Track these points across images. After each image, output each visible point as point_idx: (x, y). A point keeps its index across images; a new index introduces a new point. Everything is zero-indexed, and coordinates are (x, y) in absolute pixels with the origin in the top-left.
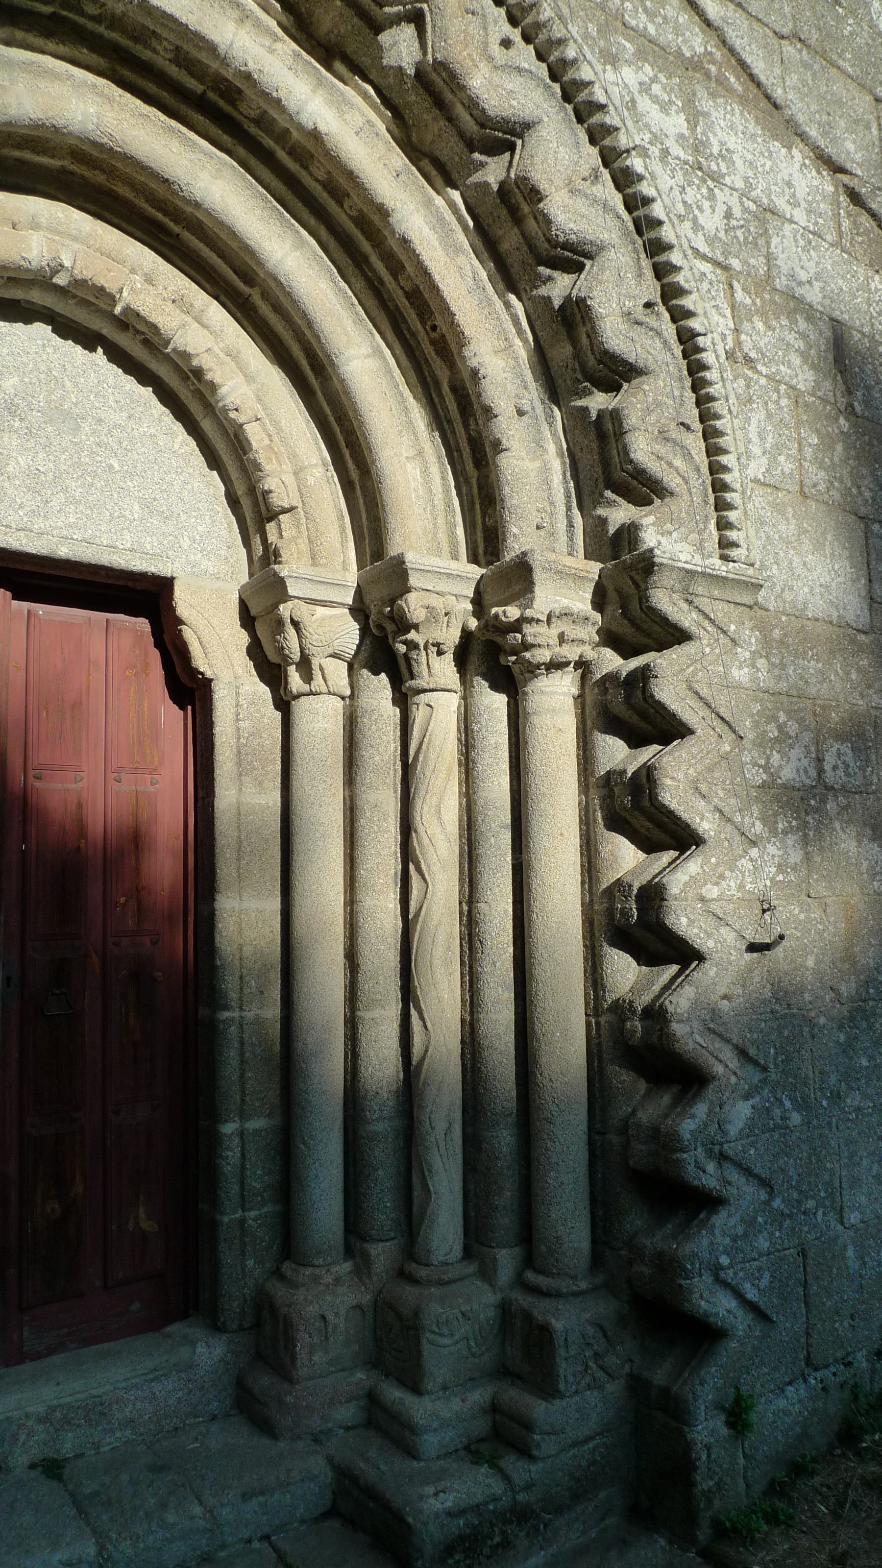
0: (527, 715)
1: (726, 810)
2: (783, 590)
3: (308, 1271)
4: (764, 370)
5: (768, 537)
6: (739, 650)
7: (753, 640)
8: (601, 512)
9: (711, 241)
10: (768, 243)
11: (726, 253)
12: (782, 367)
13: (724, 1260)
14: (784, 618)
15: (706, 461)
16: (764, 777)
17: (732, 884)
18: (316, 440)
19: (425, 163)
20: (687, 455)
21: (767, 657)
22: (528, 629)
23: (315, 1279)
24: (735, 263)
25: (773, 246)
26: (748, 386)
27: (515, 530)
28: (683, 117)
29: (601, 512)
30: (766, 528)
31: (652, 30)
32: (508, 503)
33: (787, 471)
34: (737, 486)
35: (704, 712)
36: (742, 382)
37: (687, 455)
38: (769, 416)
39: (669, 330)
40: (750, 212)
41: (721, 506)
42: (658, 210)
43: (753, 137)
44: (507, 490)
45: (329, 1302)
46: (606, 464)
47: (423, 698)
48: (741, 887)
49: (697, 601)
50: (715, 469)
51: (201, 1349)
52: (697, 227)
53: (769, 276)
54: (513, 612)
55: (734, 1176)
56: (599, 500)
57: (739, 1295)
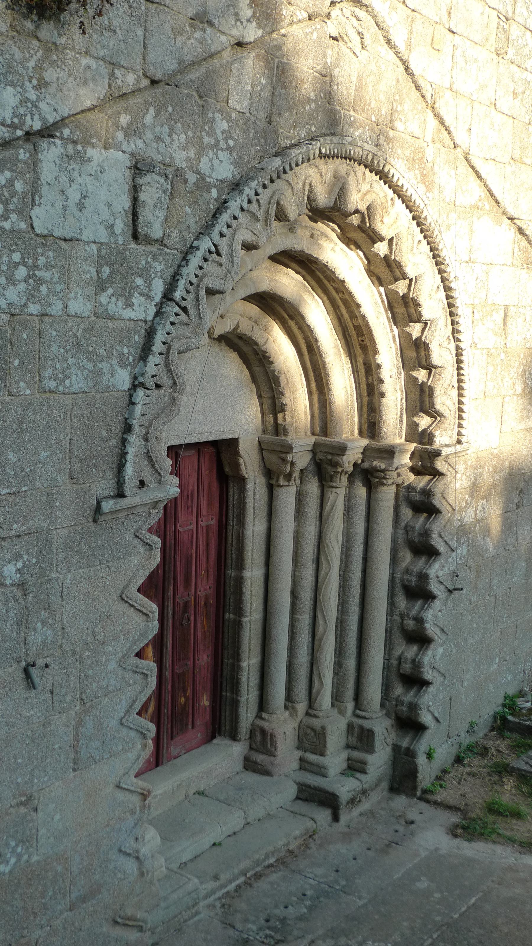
0: (377, 500)
3: (275, 716)
8: (415, 419)
13: (431, 703)
15: (457, 399)
18: (301, 375)
19: (374, 279)
22: (387, 473)
23: (278, 719)
27: (385, 430)
29: (415, 419)
32: (384, 418)
39: (453, 344)
41: (460, 418)
44: (383, 413)
45: (284, 726)
46: (422, 402)
47: (334, 490)
50: (460, 403)
51: (235, 748)
54: (383, 466)
55: (436, 674)
56: (417, 414)
57: (433, 715)
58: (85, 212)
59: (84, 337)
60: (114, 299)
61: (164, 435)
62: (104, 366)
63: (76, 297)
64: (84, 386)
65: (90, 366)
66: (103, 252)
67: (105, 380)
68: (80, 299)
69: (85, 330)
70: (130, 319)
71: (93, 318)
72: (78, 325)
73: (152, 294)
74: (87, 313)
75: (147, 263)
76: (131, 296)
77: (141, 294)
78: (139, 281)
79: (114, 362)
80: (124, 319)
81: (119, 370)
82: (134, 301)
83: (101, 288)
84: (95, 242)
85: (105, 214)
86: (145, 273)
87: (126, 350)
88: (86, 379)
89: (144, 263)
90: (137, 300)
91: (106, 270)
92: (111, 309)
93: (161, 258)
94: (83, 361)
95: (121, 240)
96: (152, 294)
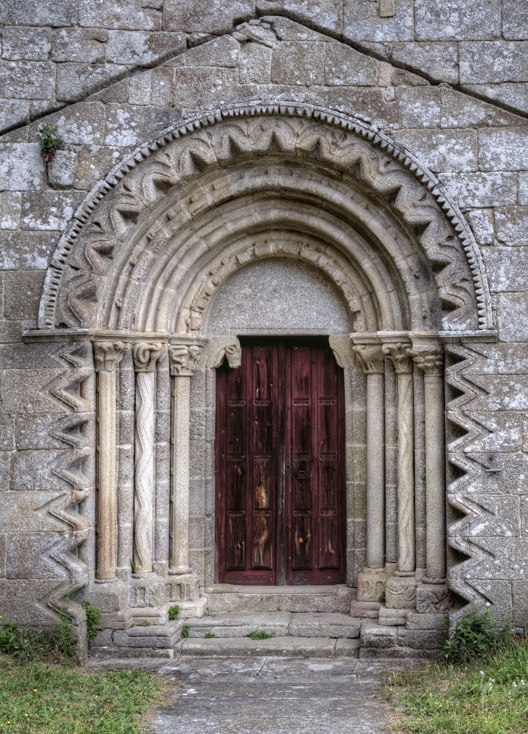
1: (478, 420)
2: (515, 333)
4: (510, 244)
5: (508, 314)
6: (489, 360)
7: (496, 355)
9: (482, 201)
10: (518, 187)
11: (491, 202)
12: (522, 239)
14: (515, 344)
16: (499, 407)
17: (478, 447)
20: (466, 290)
21: (504, 361)
24: (496, 204)
25: (521, 188)
26: (500, 254)
28: (471, 152)
30: (507, 310)
31: (455, 123)
33: (522, 283)
34: (484, 300)
35: (469, 386)
36: (497, 253)
37: (466, 290)
38: (512, 262)
40: (507, 178)
42: (446, 206)
43: (514, 141)
48: (483, 448)
49: (466, 345)
52: (474, 196)
53: (517, 203)
58: (13, 176)
59: (13, 240)
60: (34, 220)
61: (126, 305)
62: (28, 256)
63: (7, 220)
64: (12, 266)
65: (17, 256)
66: (25, 196)
67: (29, 263)
68: (10, 221)
69: (14, 237)
70: (46, 230)
71: (20, 230)
72: (8, 234)
73: (64, 215)
74: (15, 228)
75: (59, 198)
76: (47, 218)
77: (56, 216)
78: (54, 209)
79: (36, 254)
80: (41, 230)
81: (39, 258)
82: (49, 220)
83: (24, 213)
84: (19, 191)
85: (27, 175)
86: (59, 205)
87: (44, 247)
88: (15, 263)
89: (57, 199)
90: (52, 219)
91: (28, 205)
92: (32, 225)
93: (71, 196)
94: (12, 253)
95: (38, 188)
96: (64, 215)
